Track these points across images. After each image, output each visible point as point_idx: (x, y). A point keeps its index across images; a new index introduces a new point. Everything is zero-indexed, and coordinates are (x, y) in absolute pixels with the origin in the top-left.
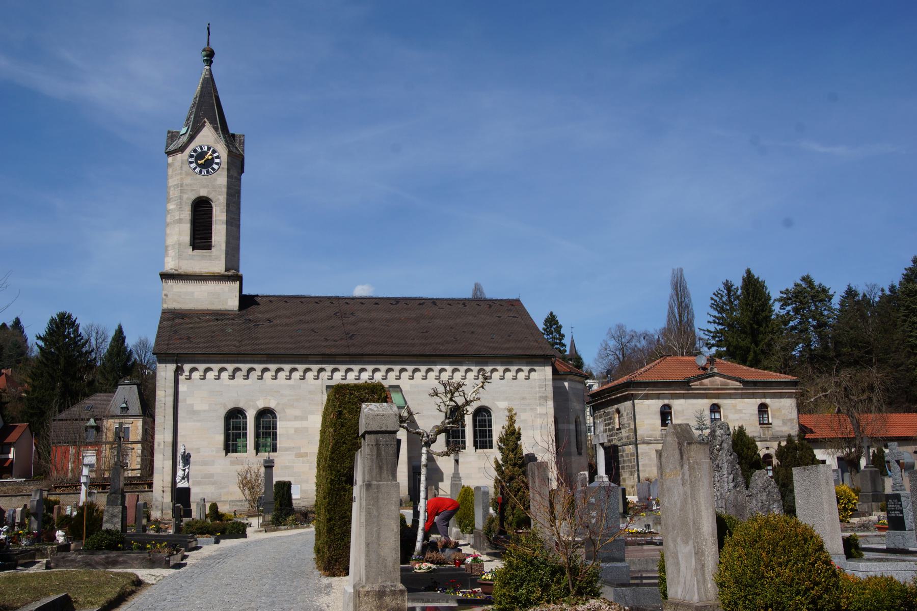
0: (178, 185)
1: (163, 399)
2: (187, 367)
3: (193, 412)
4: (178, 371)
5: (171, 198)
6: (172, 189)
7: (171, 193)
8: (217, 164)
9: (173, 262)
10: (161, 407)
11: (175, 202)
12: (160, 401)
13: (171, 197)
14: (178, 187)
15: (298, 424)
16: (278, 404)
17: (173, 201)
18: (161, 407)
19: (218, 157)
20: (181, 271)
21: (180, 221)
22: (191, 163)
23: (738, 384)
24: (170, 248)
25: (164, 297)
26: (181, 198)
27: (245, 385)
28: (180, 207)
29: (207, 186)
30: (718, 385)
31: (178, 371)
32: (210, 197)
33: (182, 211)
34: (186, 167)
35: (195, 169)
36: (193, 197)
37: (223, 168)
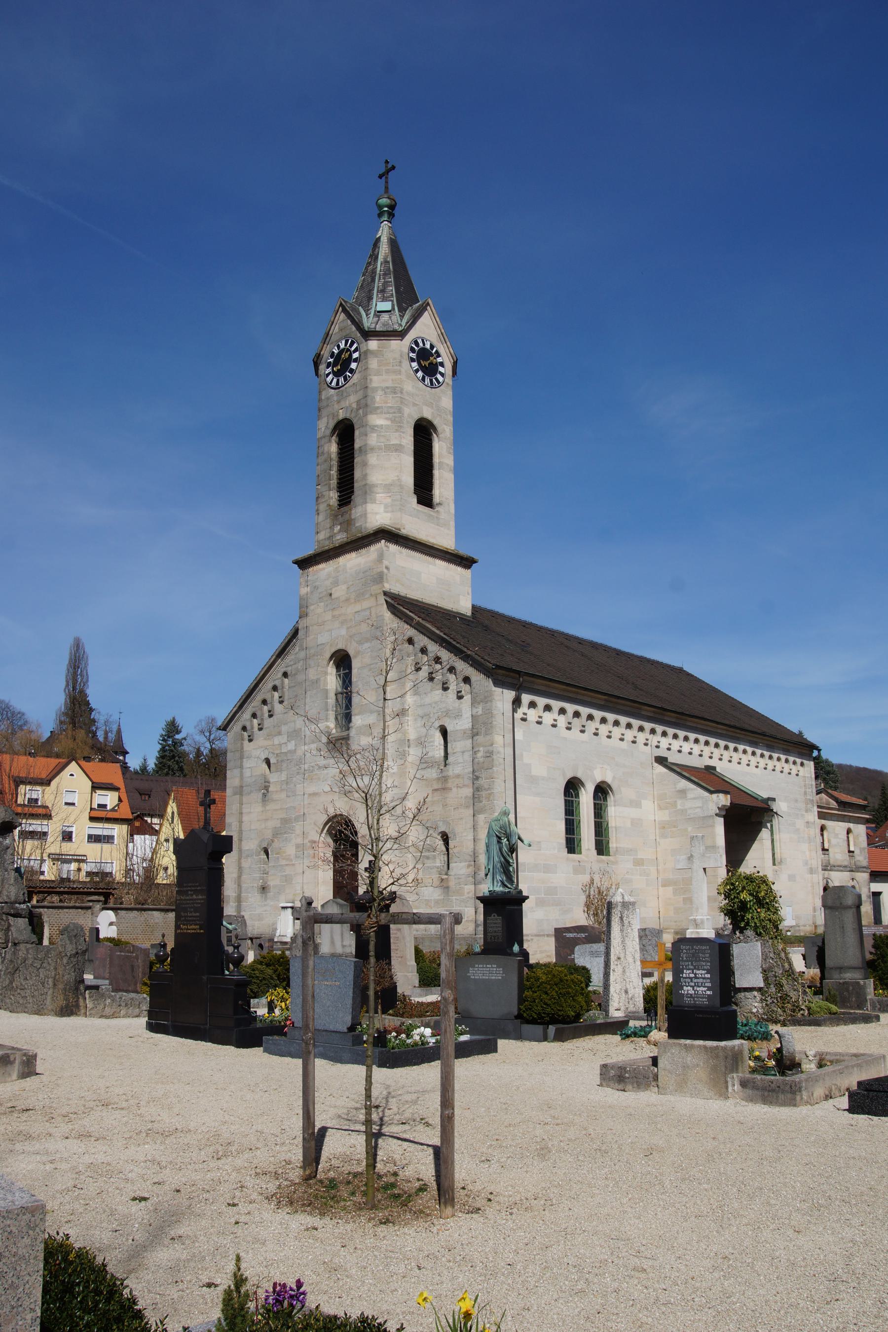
0: (395, 388)
1: (501, 750)
2: (526, 698)
3: (533, 780)
4: (517, 702)
5: (378, 408)
6: (380, 392)
7: (378, 398)
8: (442, 375)
9: (389, 515)
10: (500, 764)
11: (388, 416)
12: (498, 753)
13: (377, 405)
14: (395, 393)
15: (633, 813)
16: (614, 778)
17: (381, 413)
18: (500, 764)
19: (442, 364)
20: (404, 532)
21: (398, 448)
22: (412, 360)
23: (835, 803)
24: (379, 490)
25: (385, 571)
26: (400, 410)
27: (583, 742)
28: (397, 423)
29: (430, 405)
30: (823, 803)
31: (517, 702)
32: (435, 422)
33: (403, 433)
34: (406, 363)
35: (417, 371)
36: (416, 417)
37: (448, 384)
